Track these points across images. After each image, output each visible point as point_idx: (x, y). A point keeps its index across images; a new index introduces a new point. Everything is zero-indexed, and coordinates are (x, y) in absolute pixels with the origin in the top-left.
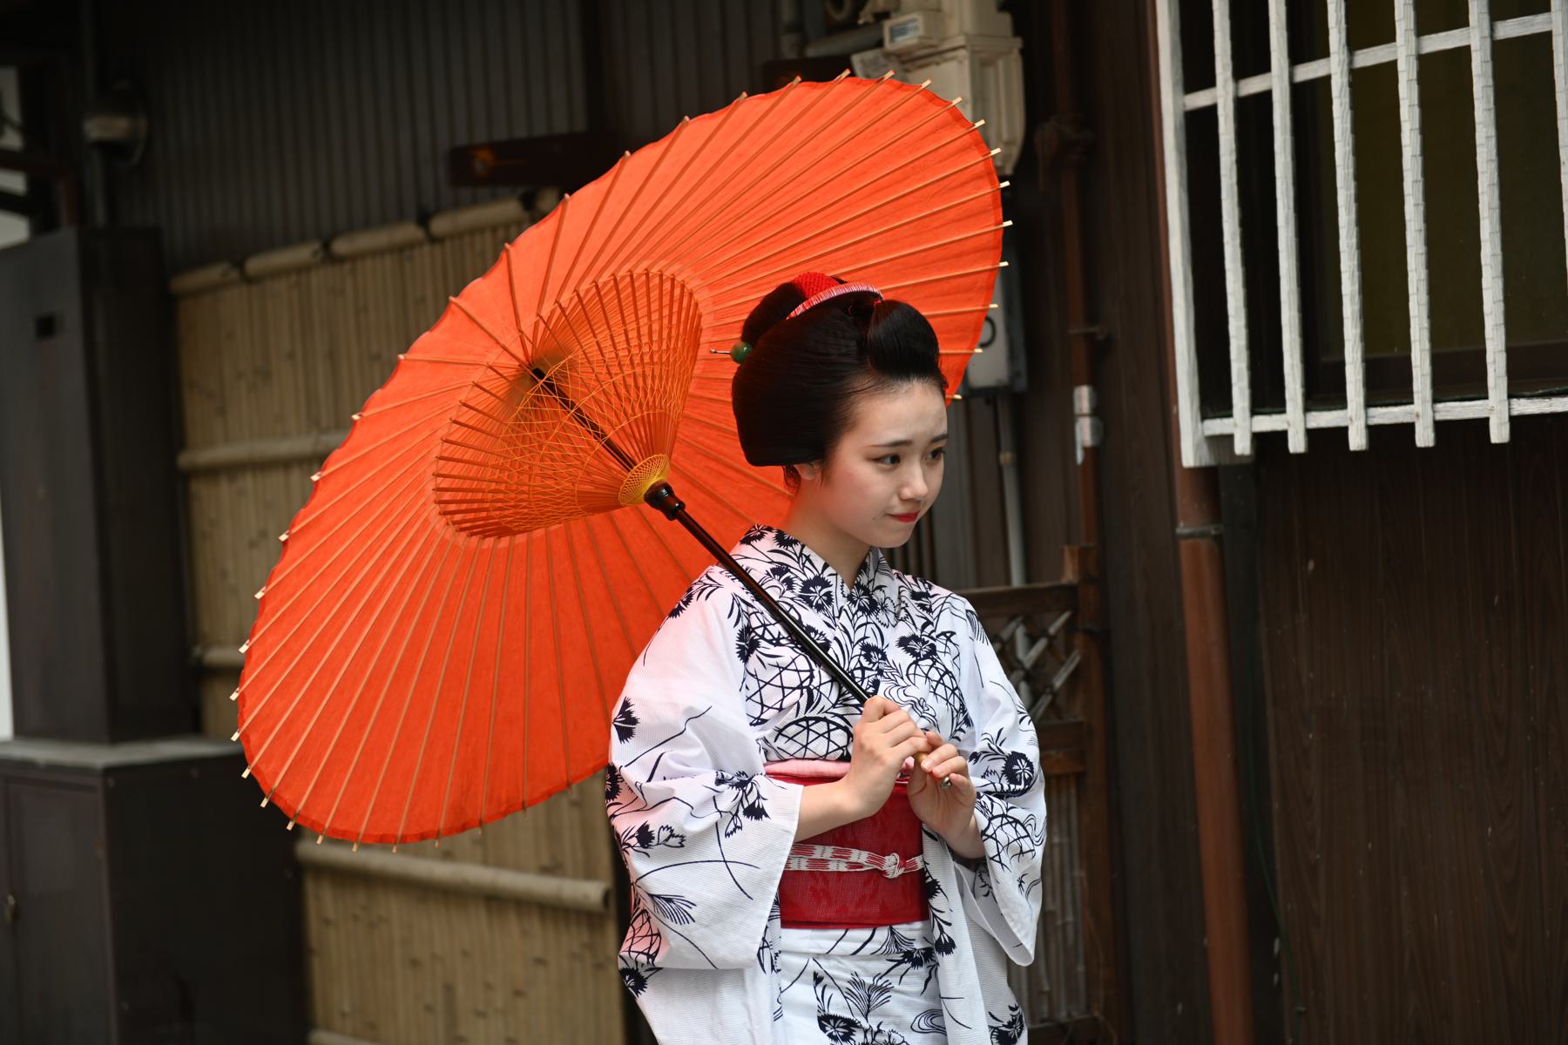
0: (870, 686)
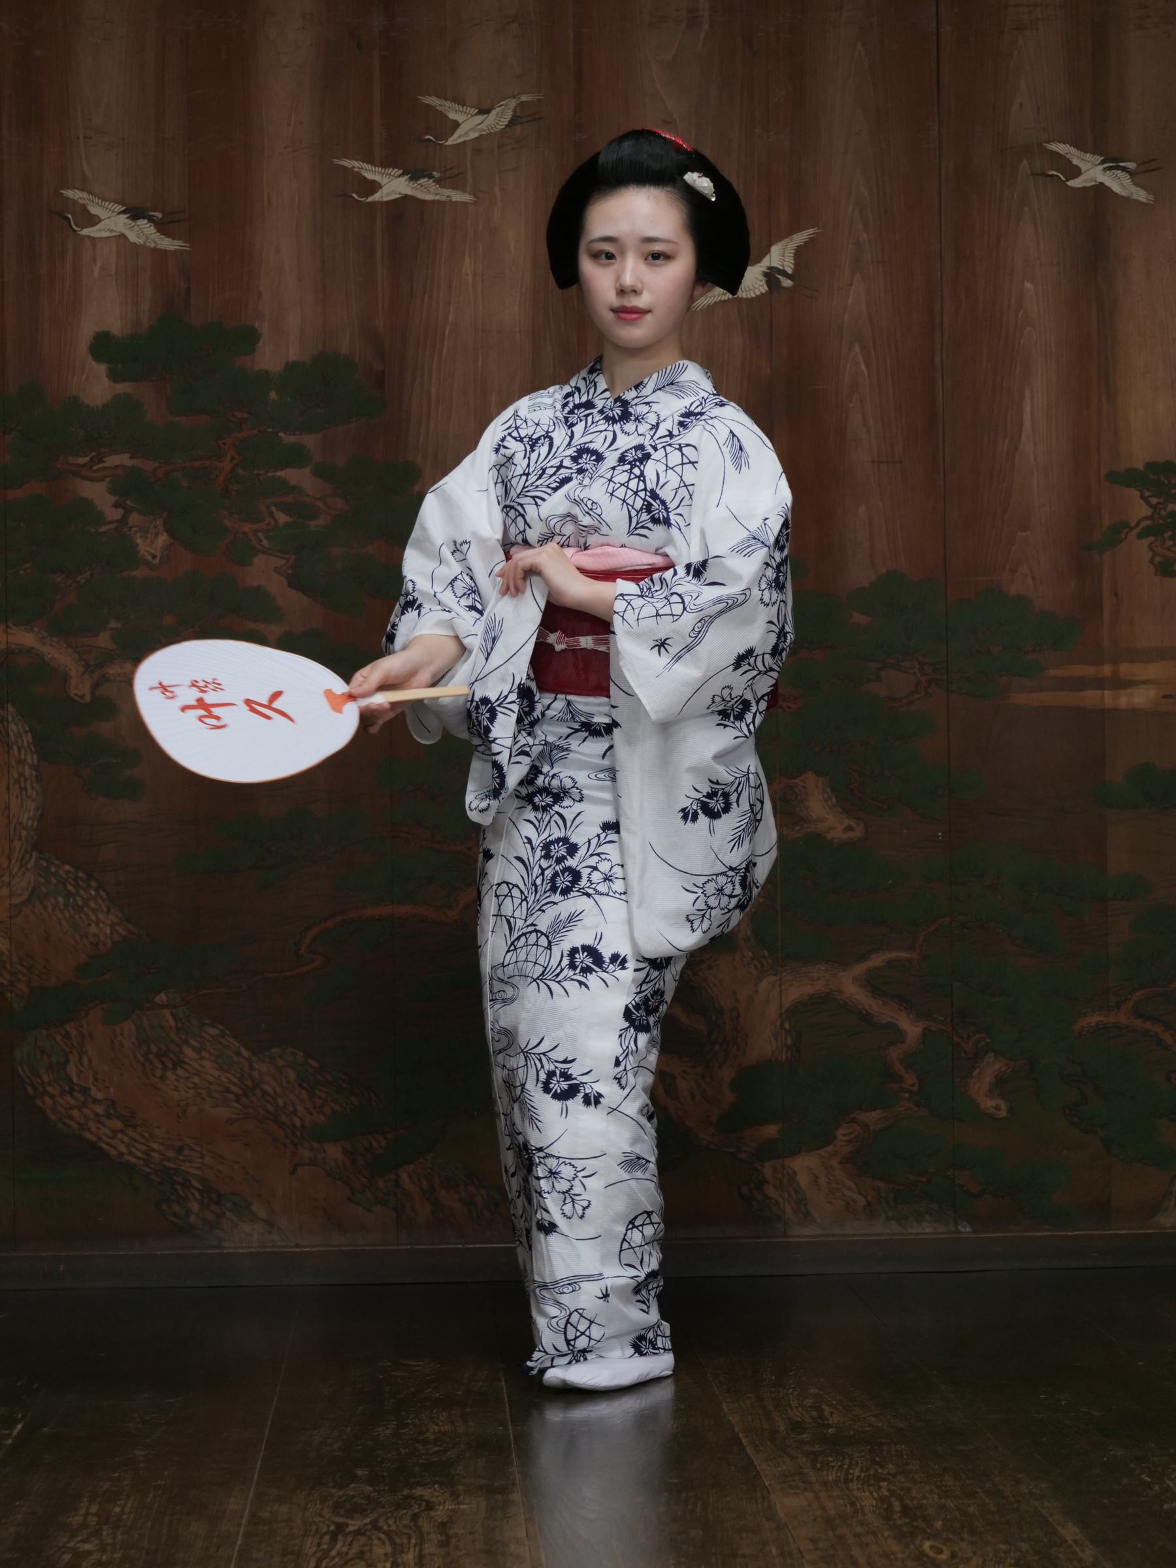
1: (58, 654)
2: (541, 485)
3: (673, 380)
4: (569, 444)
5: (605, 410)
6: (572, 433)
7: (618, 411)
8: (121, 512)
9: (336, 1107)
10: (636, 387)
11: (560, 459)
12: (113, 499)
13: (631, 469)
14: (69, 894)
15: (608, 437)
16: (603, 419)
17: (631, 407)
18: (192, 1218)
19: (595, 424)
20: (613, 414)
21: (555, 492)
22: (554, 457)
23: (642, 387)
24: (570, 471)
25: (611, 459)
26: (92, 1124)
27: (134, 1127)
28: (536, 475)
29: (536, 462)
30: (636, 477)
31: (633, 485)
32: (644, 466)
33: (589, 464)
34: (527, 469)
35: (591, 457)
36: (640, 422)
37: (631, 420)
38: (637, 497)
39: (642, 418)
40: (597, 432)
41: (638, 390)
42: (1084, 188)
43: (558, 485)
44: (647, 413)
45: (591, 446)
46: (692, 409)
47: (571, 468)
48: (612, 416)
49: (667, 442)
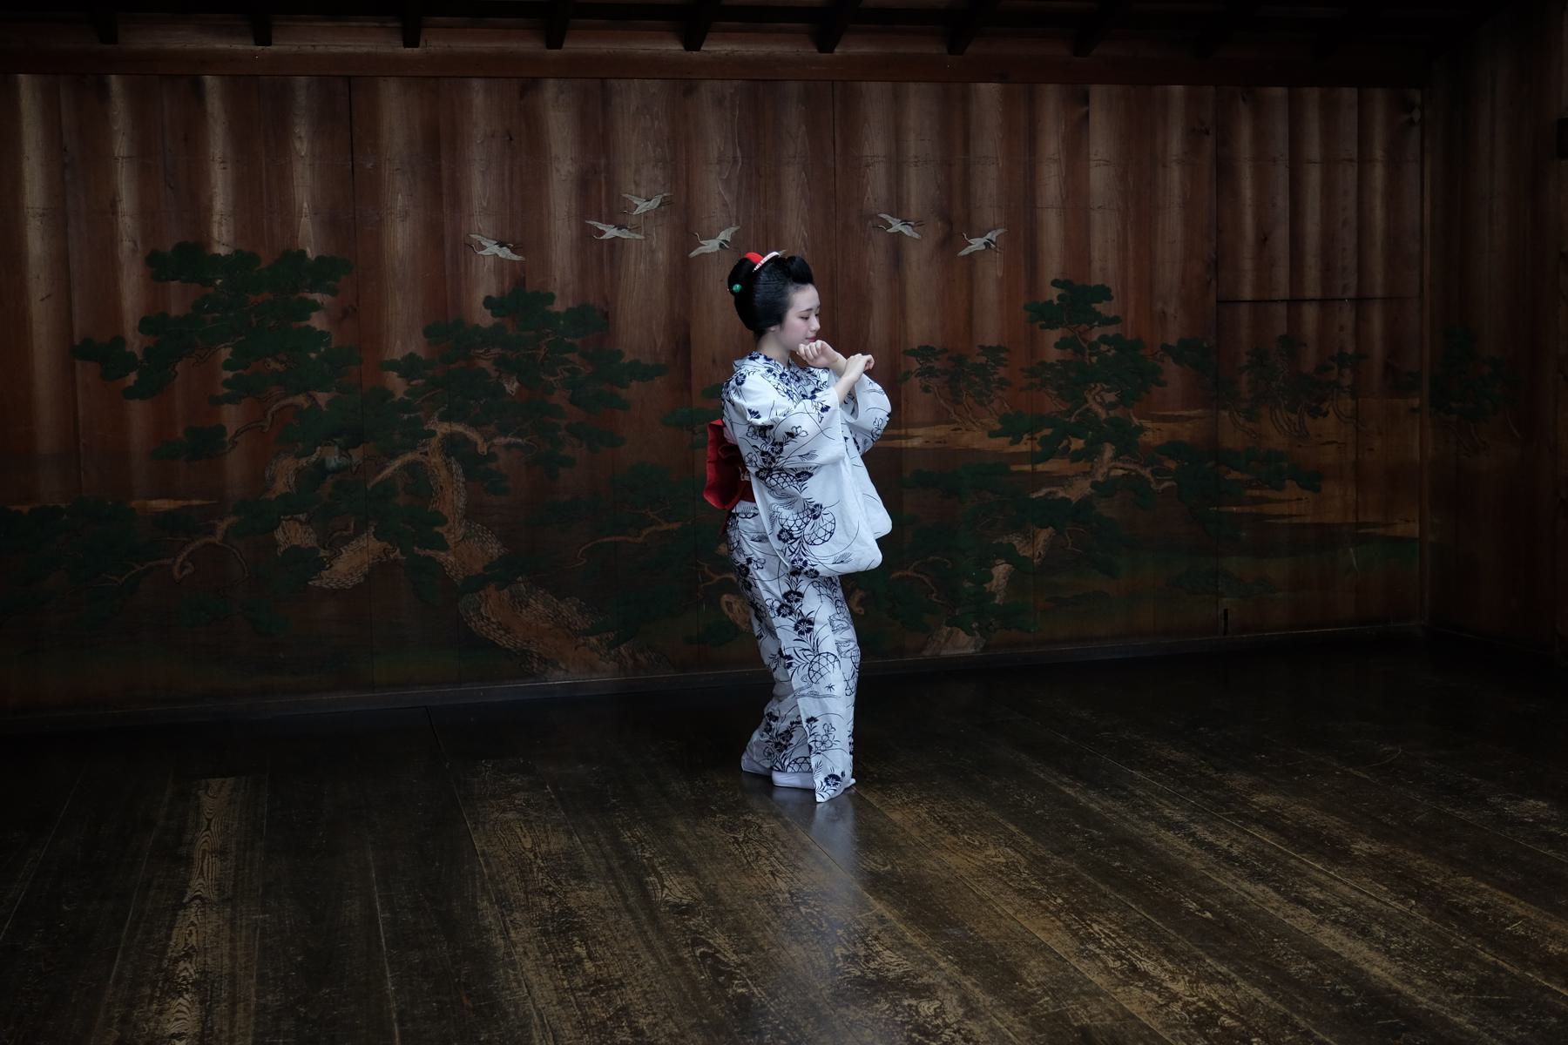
1: (473, 435)
8: (497, 374)
9: (594, 622)
12: (494, 367)
14: (479, 537)
18: (535, 670)
26: (492, 633)
27: (509, 633)
42: (894, 233)
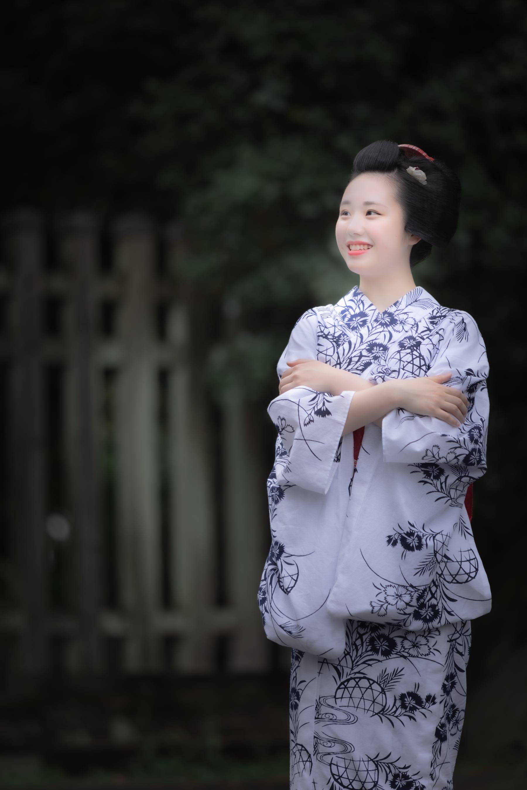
0: (368, 646)
2: (352, 369)
3: (416, 299)
4: (362, 341)
5: (379, 319)
6: (361, 334)
7: (387, 320)
10: (395, 304)
11: (360, 351)
13: (412, 352)
15: (386, 335)
16: (379, 325)
17: (396, 316)
19: (375, 329)
20: (385, 321)
21: (362, 372)
22: (354, 350)
23: (399, 304)
24: (369, 358)
25: (394, 348)
28: (346, 363)
29: (344, 354)
30: (417, 357)
31: (417, 362)
32: (419, 350)
33: (380, 353)
34: (339, 360)
35: (379, 348)
36: (404, 324)
37: (398, 323)
38: (421, 370)
39: (405, 322)
40: (378, 333)
41: (397, 306)
43: (364, 367)
44: (407, 318)
45: (377, 341)
46: (434, 314)
47: (369, 357)
48: (384, 322)
49: (428, 334)
